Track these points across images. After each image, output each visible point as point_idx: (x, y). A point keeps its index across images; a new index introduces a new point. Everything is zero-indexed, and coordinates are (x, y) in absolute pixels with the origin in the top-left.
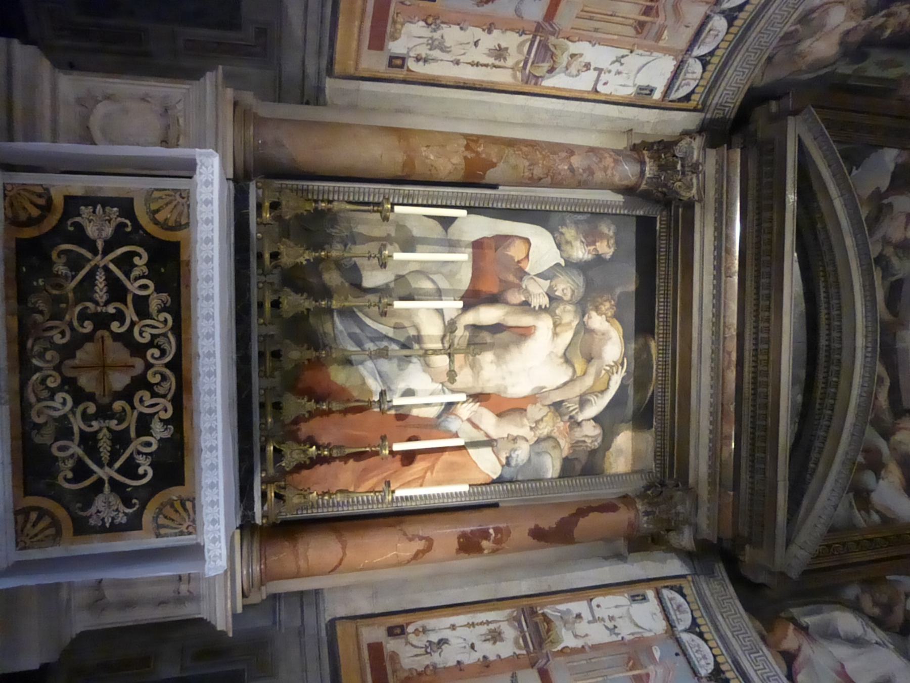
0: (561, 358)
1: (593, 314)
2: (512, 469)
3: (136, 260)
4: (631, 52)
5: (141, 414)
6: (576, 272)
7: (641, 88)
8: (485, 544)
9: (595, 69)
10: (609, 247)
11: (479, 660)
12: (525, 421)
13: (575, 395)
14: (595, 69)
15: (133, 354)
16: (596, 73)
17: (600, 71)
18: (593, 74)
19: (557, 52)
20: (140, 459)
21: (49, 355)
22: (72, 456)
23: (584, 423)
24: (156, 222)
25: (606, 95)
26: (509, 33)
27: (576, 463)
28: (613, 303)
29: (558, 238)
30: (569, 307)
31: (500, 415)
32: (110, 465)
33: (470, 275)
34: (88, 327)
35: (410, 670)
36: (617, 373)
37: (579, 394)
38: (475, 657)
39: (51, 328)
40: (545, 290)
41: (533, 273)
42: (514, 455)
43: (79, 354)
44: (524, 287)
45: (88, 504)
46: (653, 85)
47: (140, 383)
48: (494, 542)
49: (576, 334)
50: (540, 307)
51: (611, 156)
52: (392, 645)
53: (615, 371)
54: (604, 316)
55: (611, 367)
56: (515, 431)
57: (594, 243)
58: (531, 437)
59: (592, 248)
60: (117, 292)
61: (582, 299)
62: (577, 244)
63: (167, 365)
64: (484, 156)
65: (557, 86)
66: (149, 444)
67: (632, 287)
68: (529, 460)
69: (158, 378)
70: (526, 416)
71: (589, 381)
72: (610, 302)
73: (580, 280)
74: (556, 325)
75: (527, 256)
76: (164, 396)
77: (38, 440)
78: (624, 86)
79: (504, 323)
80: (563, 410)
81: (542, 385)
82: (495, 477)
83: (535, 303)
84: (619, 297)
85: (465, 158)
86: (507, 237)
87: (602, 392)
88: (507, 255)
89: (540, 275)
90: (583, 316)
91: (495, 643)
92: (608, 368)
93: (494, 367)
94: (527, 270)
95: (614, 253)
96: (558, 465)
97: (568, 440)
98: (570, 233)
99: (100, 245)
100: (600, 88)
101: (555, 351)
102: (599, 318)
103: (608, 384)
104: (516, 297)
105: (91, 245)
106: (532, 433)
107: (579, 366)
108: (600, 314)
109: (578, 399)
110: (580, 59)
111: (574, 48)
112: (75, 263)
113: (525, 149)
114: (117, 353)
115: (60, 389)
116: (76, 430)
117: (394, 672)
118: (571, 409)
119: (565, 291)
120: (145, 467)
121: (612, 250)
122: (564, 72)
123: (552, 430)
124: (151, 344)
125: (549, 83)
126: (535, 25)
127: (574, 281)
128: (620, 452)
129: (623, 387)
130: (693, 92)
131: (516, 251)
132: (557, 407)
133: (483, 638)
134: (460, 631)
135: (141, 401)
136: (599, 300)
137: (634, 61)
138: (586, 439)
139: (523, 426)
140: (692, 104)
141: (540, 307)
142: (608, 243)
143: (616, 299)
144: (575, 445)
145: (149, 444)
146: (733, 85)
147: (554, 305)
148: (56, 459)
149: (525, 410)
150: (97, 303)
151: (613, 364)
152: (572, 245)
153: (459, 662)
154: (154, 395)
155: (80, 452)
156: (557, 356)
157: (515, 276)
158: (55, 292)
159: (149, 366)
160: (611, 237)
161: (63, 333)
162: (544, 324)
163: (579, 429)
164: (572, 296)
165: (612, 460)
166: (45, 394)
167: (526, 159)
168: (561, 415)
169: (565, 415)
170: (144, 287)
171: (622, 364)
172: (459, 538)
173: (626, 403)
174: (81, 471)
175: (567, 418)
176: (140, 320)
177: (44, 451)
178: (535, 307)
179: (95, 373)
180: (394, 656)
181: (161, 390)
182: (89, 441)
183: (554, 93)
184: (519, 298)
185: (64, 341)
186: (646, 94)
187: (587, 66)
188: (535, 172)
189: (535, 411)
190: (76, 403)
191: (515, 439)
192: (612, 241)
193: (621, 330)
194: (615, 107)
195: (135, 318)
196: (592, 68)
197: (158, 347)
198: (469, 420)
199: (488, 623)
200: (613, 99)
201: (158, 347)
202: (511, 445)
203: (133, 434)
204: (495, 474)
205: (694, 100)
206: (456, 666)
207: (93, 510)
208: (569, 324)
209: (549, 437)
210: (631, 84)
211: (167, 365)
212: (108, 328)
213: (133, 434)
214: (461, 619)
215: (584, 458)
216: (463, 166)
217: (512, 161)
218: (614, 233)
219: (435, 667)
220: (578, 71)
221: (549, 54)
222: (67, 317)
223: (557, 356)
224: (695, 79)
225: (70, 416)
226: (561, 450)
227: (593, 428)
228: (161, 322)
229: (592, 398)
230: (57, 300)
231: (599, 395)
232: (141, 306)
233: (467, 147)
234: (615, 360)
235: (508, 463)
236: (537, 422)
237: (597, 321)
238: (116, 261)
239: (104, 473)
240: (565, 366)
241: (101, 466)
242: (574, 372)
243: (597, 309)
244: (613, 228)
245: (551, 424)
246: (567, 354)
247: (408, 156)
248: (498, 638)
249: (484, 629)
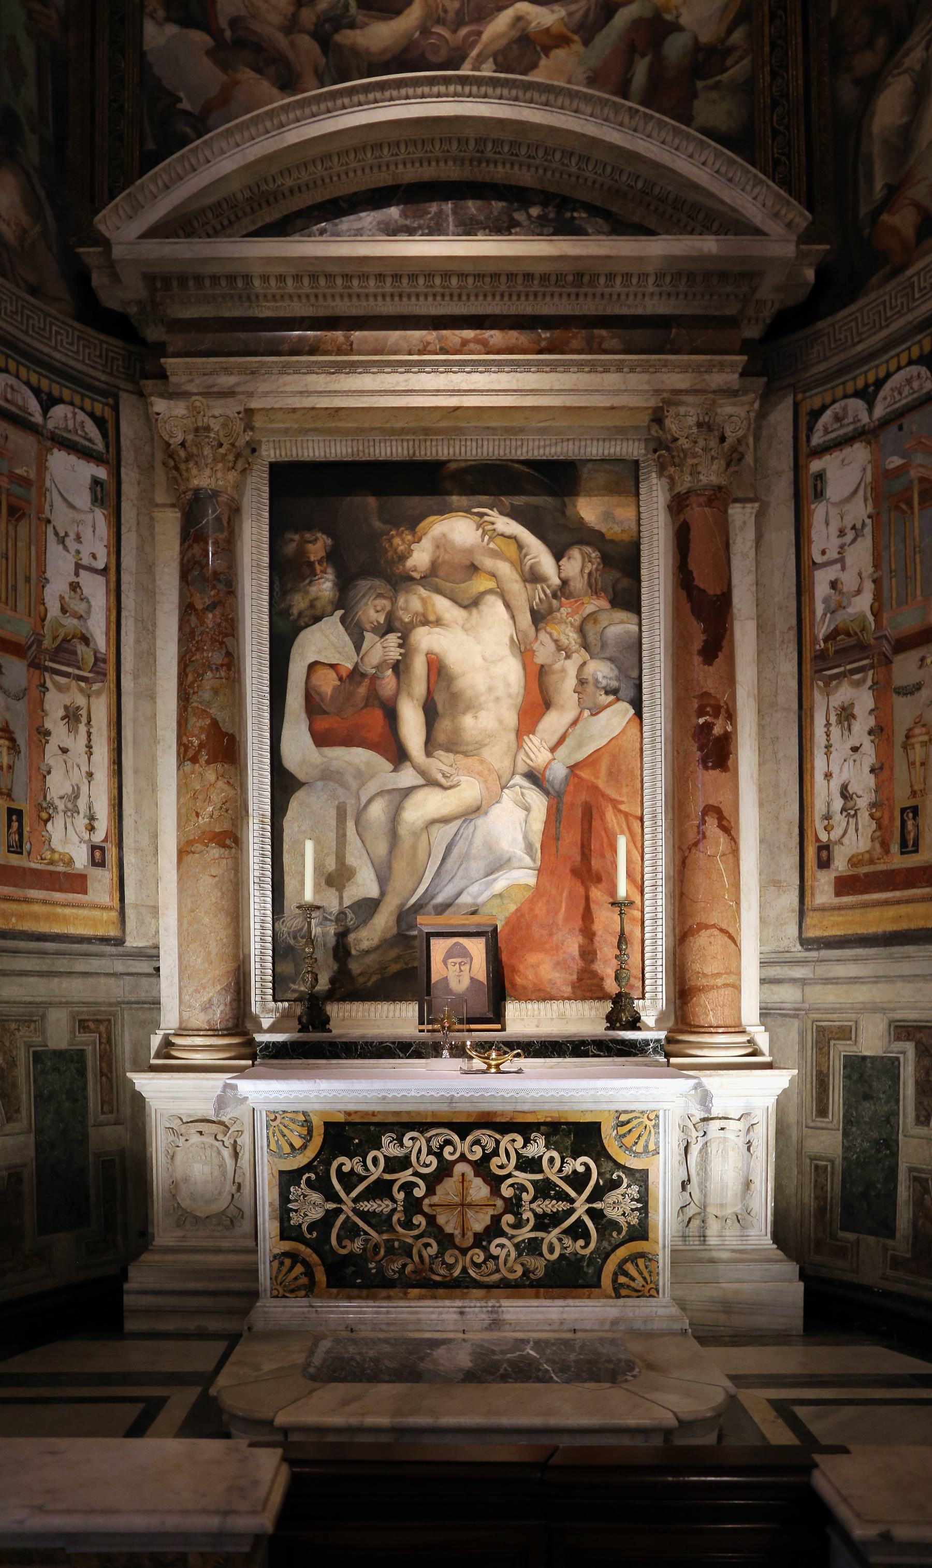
0: (470, 614)
1: (410, 563)
2: (623, 686)
3: (346, 1169)
4: (49, 521)
5: (517, 1168)
6: (351, 594)
7: (95, 500)
8: (717, 731)
9: (77, 574)
10: (316, 540)
11: (872, 741)
12: (557, 666)
13: (523, 590)
14: (77, 574)
15: (450, 1175)
16: (82, 573)
17: (78, 567)
18: (86, 579)
19: (62, 633)
20: (568, 1169)
21: (451, 1261)
22: (560, 1240)
23: (563, 575)
24: (304, 1147)
25: (108, 554)
26: (47, 706)
27: (619, 587)
28: (393, 532)
29: (306, 619)
30: (401, 602)
31: (547, 704)
32: (572, 1201)
33: (360, 750)
34: (419, 1219)
35: (873, 840)
36: (493, 524)
37: (521, 584)
38: (868, 748)
39: (421, 1256)
40: (377, 638)
41: (355, 658)
42: (604, 682)
43: (449, 1229)
44: (373, 671)
45: (615, 1225)
46: (88, 481)
47: (481, 1167)
48: (716, 715)
49: (439, 591)
50: (400, 646)
51: (190, 546)
52: (840, 864)
53: (490, 527)
54: (413, 547)
55: (484, 533)
56: (570, 682)
57: (311, 565)
58: (580, 656)
59: (318, 568)
60: (381, 1189)
61: (389, 581)
62: (313, 590)
63: (463, 1138)
64: (203, 737)
65: (104, 629)
66: (552, 1160)
67: (372, 502)
68: (611, 660)
69: (477, 1148)
70: (550, 666)
71: (504, 569)
72: (393, 537)
73: (364, 585)
74: (426, 622)
75: (333, 666)
76: (498, 1142)
77: (540, 1273)
78: (94, 527)
79: (422, 700)
80: (543, 608)
81: (507, 641)
82: (632, 711)
83: (395, 654)
84: (385, 522)
85: (208, 762)
87: (520, 546)
88: (332, 696)
89: (358, 647)
90: (412, 579)
91: (854, 716)
92: (487, 538)
93: (483, 714)
94: (350, 666)
95: (323, 533)
96: (621, 615)
97: (586, 600)
98: (299, 603)
99: (331, 1206)
100: (100, 565)
101: (461, 622)
102: (415, 555)
103: (509, 537)
104: (388, 680)
105: (331, 1215)
106: (575, 655)
107: (482, 584)
108: (410, 552)
109: (528, 586)
110: (67, 599)
111: (54, 610)
112: (351, 1231)
113: (190, 678)
114: (448, 1190)
115: (486, 1249)
116: (532, 1235)
117: (872, 862)
118: (542, 596)
119: (379, 608)
120: (577, 1165)
121: (319, 535)
122: (85, 620)
123: (572, 625)
124: (439, 1155)
125: (101, 642)
126: (32, 670)
127: (364, 596)
128: (607, 516)
129: (515, 514)
130: (91, 415)
132: (538, 618)
133: (846, 733)
134: (834, 768)
135: (502, 1167)
136: (390, 554)
137: (60, 516)
138: (587, 571)
139: (563, 670)
140: (108, 413)
141: (400, 646)
142: (310, 542)
143: (389, 527)
144: (594, 589)
145: (552, 1160)
146: (75, 349)
147: (397, 624)
148: (562, 1256)
149: (542, 666)
150: (394, 1210)
151: (481, 531)
152: (316, 599)
153: (872, 771)
154: (495, 1153)
155: (556, 1231)
156: (467, 620)
157: (360, 683)
158: (382, 1252)
159: (463, 1158)
160: (302, 537)
161: (426, 1245)
163: (572, 583)
164: (385, 598)
165: (617, 529)
166: (491, 1264)
167: (203, 675)
168: (551, 611)
169: (551, 606)
170: (375, 1161)
171: (481, 515)
172: (706, 768)
173: (536, 508)
174: (578, 1231)
175: (554, 601)
176: (411, 1166)
177: (551, 1267)
178: (401, 654)
179: (470, 1213)
180: (854, 861)
181: (491, 1145)
182: (544, 1222)
183: (113, 634)
184: (388, 680)
185: (435, 1244)
186: (102, 490)
187: (75, 587)
188: (220, 662)
189: (544, 652)
190: (502, 1234)
191: (582, 682)
192: (308, 536)
193: (431, 519)
194: (123, 538)
195: (410, 1171)
196: (76, 580)
197: (442, 1147)
198: (553, 750)
199: (828, 725)
200: (113, 542)
201: (442, 1147)
202: (590, 688)
203: (539, 1177)
204: (627, 711)
205: (103, 411)
206: (876, 776)
207: (622, 1220)
208: (424, 601)
209: (581, 631)
210: (90, 516)
211: (463, 1138)
212: (420, 1200)
213: (539, 1177)
214: (819, 763)
215: (614, 574)
216: (219, 765)
217: (207, 695)
218: (296, 533)
219: (873, 805)
220: (82, 600)
221: (66, 645)
222: (410, 1241)
223: (467, 620)
224: (75, 414)
225: (516, 1240)
226: (601, 610)
227: (572, 561)
228: (414, 1143)
229: (528, 563)
230: (390, 1250)
231: (524, 551)
232: (397, 1164)
233: (194, 760)
234: (475, 527)
235: (614, 692)
236: (559, 648)
238: (348, 1190)
239: (581, 1207)
240: (483, 607)
241: (572, 1211)
242: (491, 591)
243: (403, 557)
244: (289, 536)
245: (563, 626)
246: (466, 603)
247: (211, 841)
248: (849, 712)
249: (835, 731)
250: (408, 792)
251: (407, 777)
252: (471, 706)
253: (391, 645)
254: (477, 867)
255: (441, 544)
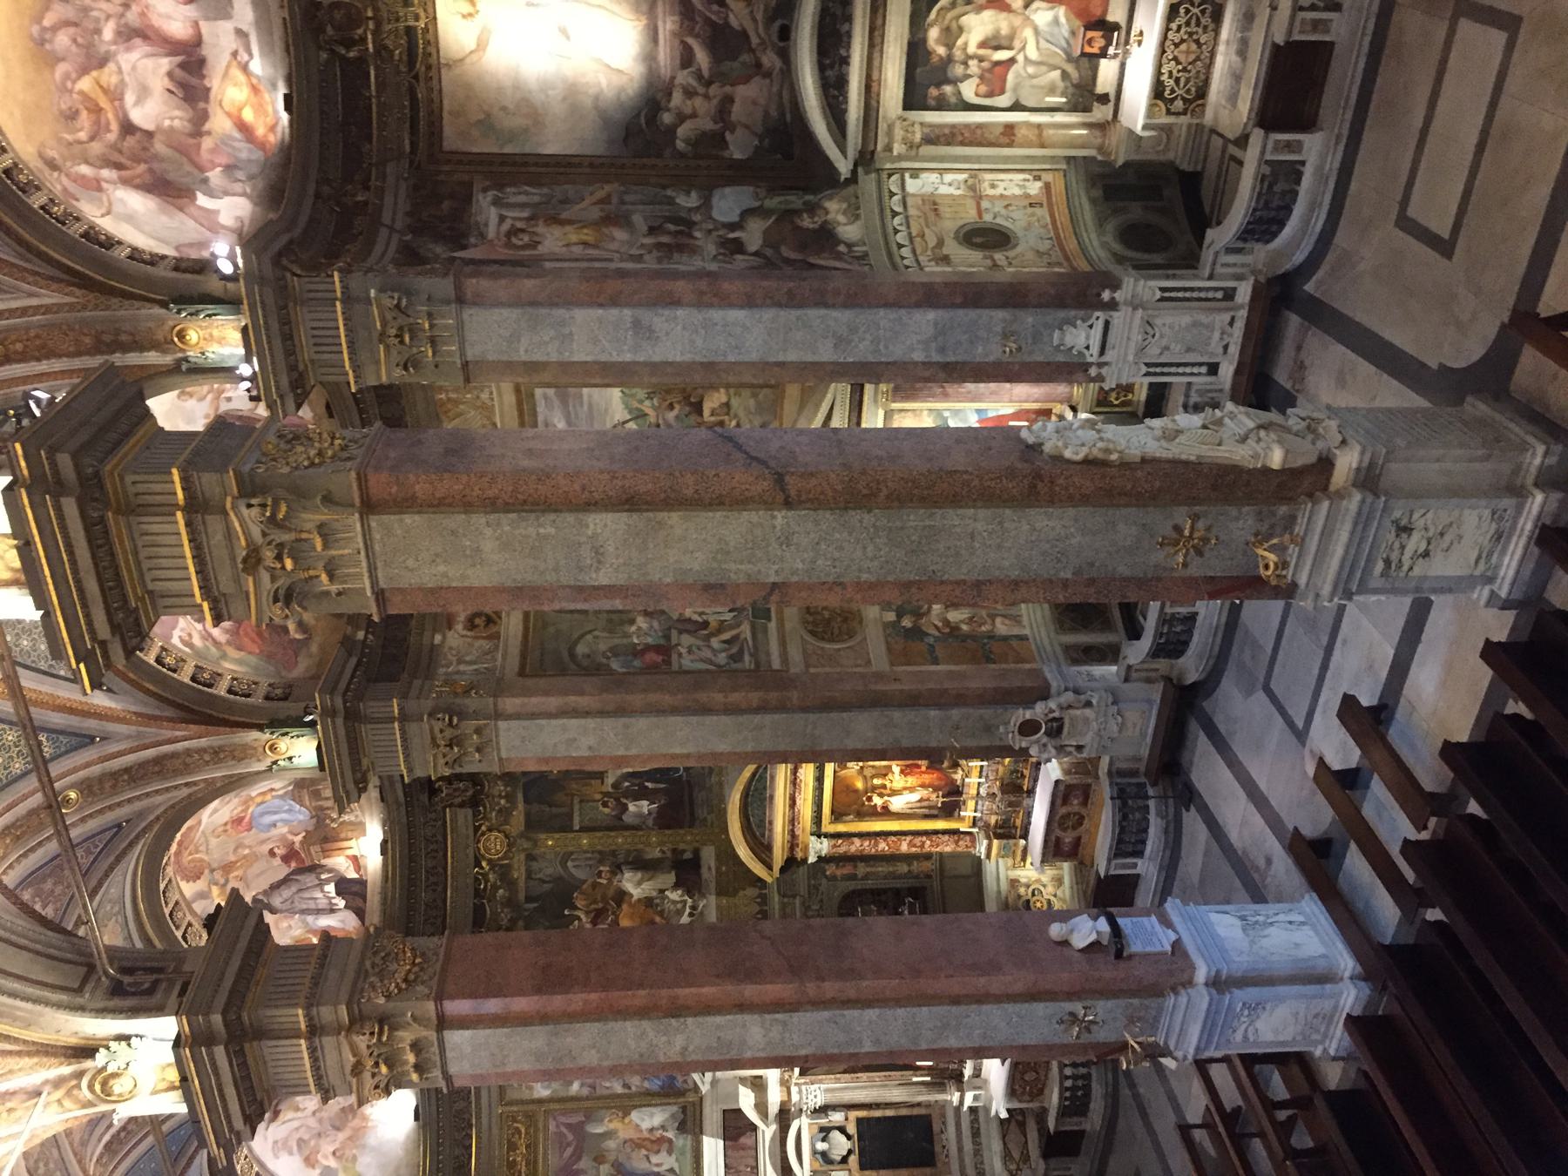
73: (950, 74)
74: (965, 49)
86: (986, 96)
89: (970, 76)
98: (953, 100)
104: (985, 65)
131: (983, 89)
162: (972, 49)
184: (985, 65)
237: (941, 51)
243: (941, 58)
250: (1026, 58)
251: (1020, 58)
252: (998, 31)
253: (974, 66)
254: (1056, 30)
255: (938, 41)
